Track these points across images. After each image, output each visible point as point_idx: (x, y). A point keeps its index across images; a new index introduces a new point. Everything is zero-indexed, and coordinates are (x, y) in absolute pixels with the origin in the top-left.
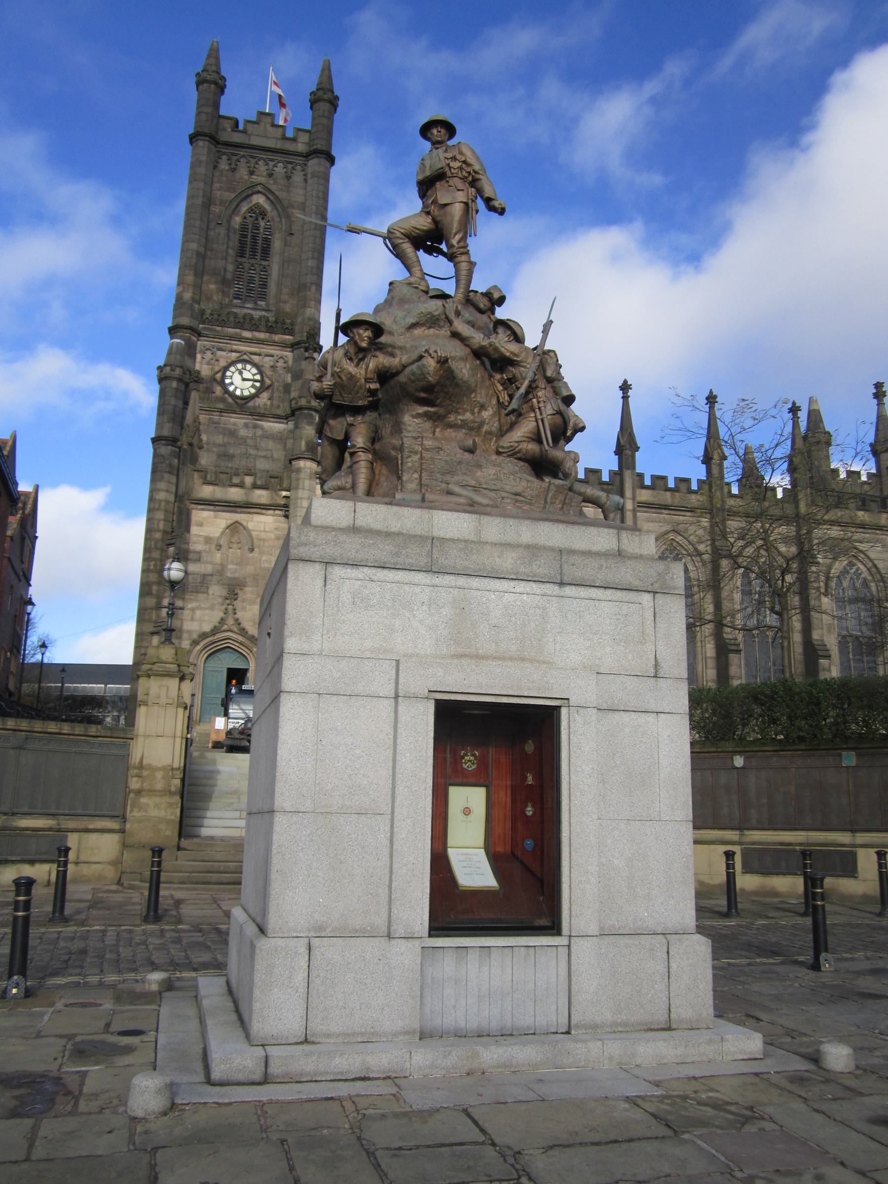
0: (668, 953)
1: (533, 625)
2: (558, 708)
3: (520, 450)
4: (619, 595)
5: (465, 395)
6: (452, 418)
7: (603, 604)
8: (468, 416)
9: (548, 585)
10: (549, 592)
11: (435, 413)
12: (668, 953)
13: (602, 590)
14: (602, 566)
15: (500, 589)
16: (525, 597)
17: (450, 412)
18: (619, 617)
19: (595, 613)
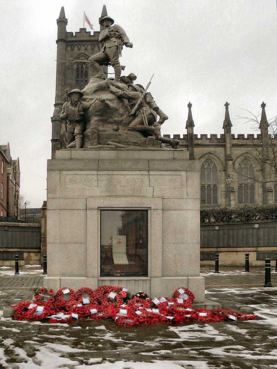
0: (188, 282)
1: (138, 185)
2: (147, 211)
3: (136, 128)
4: (172, 173)
5: (114, 112)
6: (111, 120)
7: (166, 176)
8: (116, 119)
9: (143, 172)
10: (144, 174)
11: (103, 119)
12: (188, 282)
13: (165, 172)
14: (165, 164)
15: (125, 174)
16: (135, 176)
17: (109, 118)
18: (172, 180)
19: (162, 179)
